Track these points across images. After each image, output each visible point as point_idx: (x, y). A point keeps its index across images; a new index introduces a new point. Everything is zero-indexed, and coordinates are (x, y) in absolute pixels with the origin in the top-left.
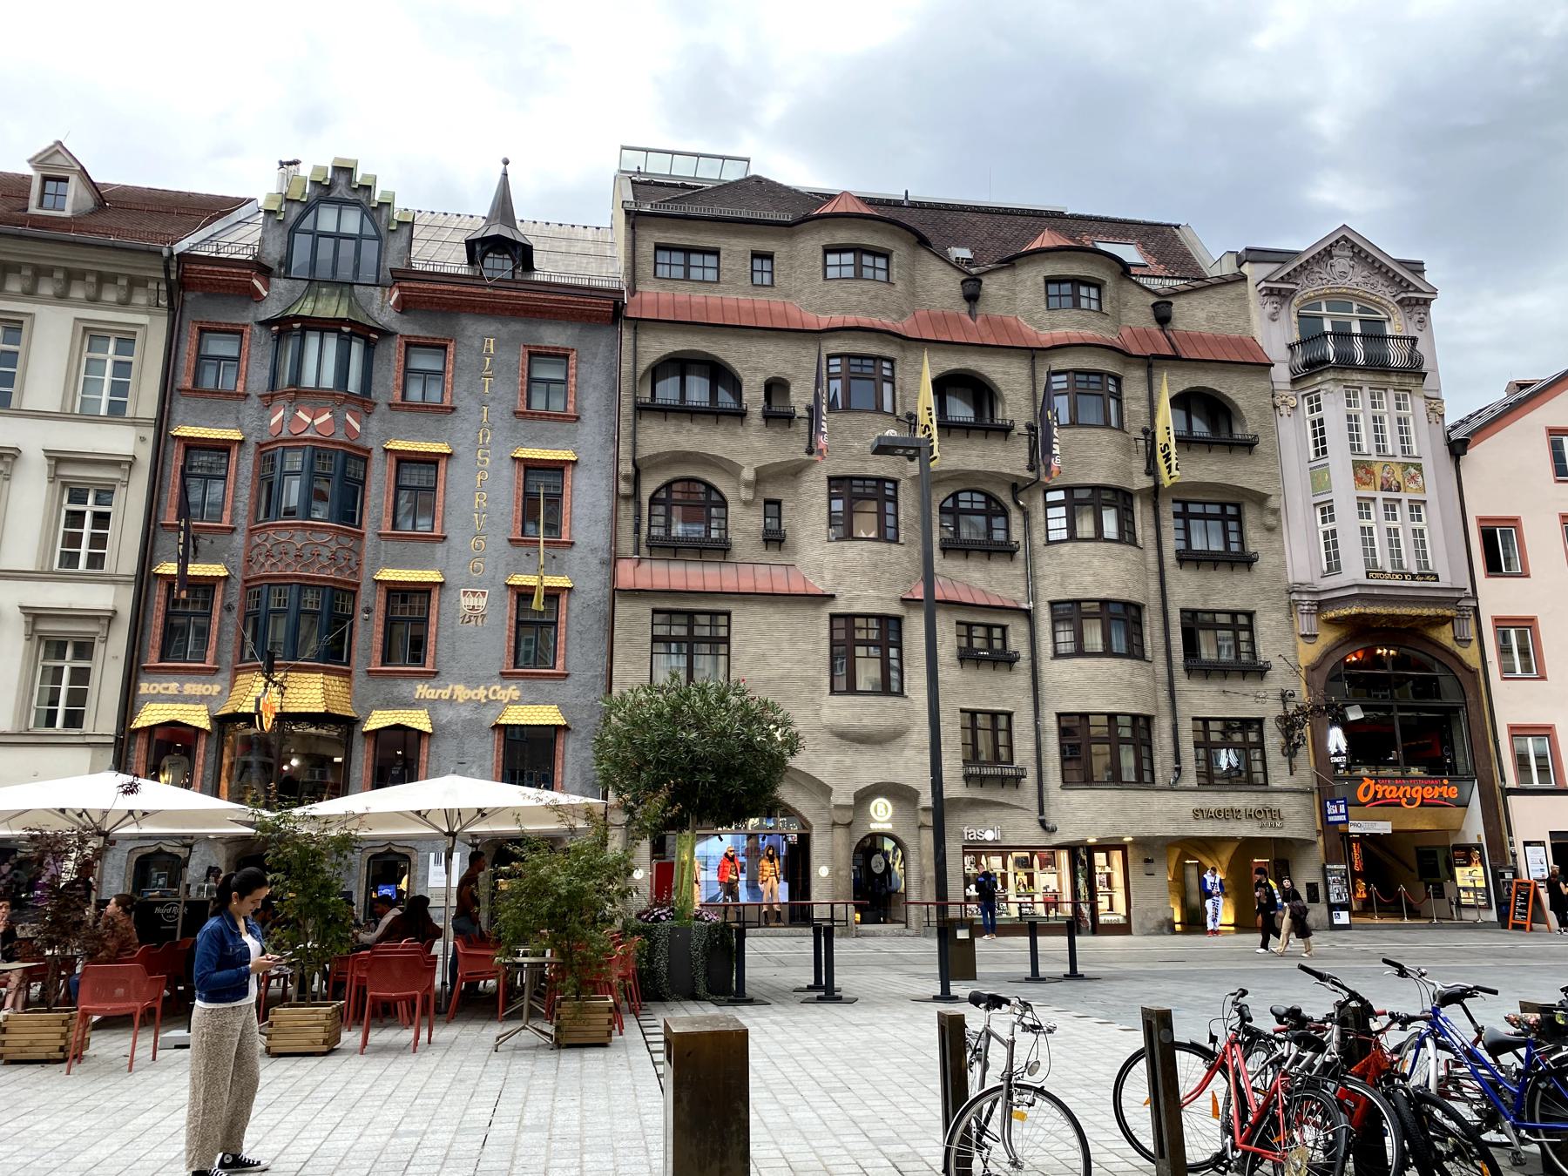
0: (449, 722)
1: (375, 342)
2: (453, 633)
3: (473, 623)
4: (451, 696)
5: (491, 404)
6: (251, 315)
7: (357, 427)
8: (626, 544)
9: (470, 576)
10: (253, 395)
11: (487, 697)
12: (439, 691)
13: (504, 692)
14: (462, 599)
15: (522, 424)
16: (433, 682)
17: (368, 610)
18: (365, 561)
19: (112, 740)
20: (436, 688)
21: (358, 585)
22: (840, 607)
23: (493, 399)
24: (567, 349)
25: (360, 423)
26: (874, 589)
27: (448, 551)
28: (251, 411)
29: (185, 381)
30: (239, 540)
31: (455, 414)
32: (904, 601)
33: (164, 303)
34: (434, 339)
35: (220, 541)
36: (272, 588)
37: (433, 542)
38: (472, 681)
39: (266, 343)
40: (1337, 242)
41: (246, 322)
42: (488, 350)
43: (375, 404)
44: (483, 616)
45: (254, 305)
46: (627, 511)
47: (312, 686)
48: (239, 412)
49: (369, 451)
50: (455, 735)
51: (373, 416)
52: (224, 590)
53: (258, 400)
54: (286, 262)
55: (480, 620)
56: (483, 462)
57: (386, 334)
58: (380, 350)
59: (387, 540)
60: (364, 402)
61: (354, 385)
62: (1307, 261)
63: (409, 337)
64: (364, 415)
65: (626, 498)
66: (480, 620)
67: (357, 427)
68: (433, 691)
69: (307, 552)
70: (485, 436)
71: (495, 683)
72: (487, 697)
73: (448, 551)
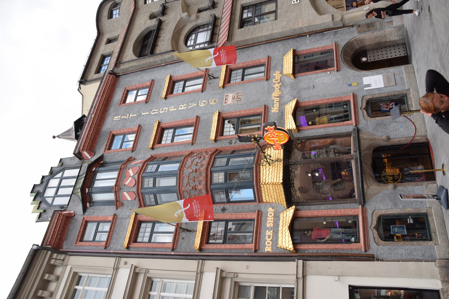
5: (141, 112)
19: (301, 262)
23: (139, 112)
24: (125, 90)
27: (204, 114)
31: (142, 125)
33: (62, 257)
42: (118, 118)
59: (196, 140)
70: (154, 112)
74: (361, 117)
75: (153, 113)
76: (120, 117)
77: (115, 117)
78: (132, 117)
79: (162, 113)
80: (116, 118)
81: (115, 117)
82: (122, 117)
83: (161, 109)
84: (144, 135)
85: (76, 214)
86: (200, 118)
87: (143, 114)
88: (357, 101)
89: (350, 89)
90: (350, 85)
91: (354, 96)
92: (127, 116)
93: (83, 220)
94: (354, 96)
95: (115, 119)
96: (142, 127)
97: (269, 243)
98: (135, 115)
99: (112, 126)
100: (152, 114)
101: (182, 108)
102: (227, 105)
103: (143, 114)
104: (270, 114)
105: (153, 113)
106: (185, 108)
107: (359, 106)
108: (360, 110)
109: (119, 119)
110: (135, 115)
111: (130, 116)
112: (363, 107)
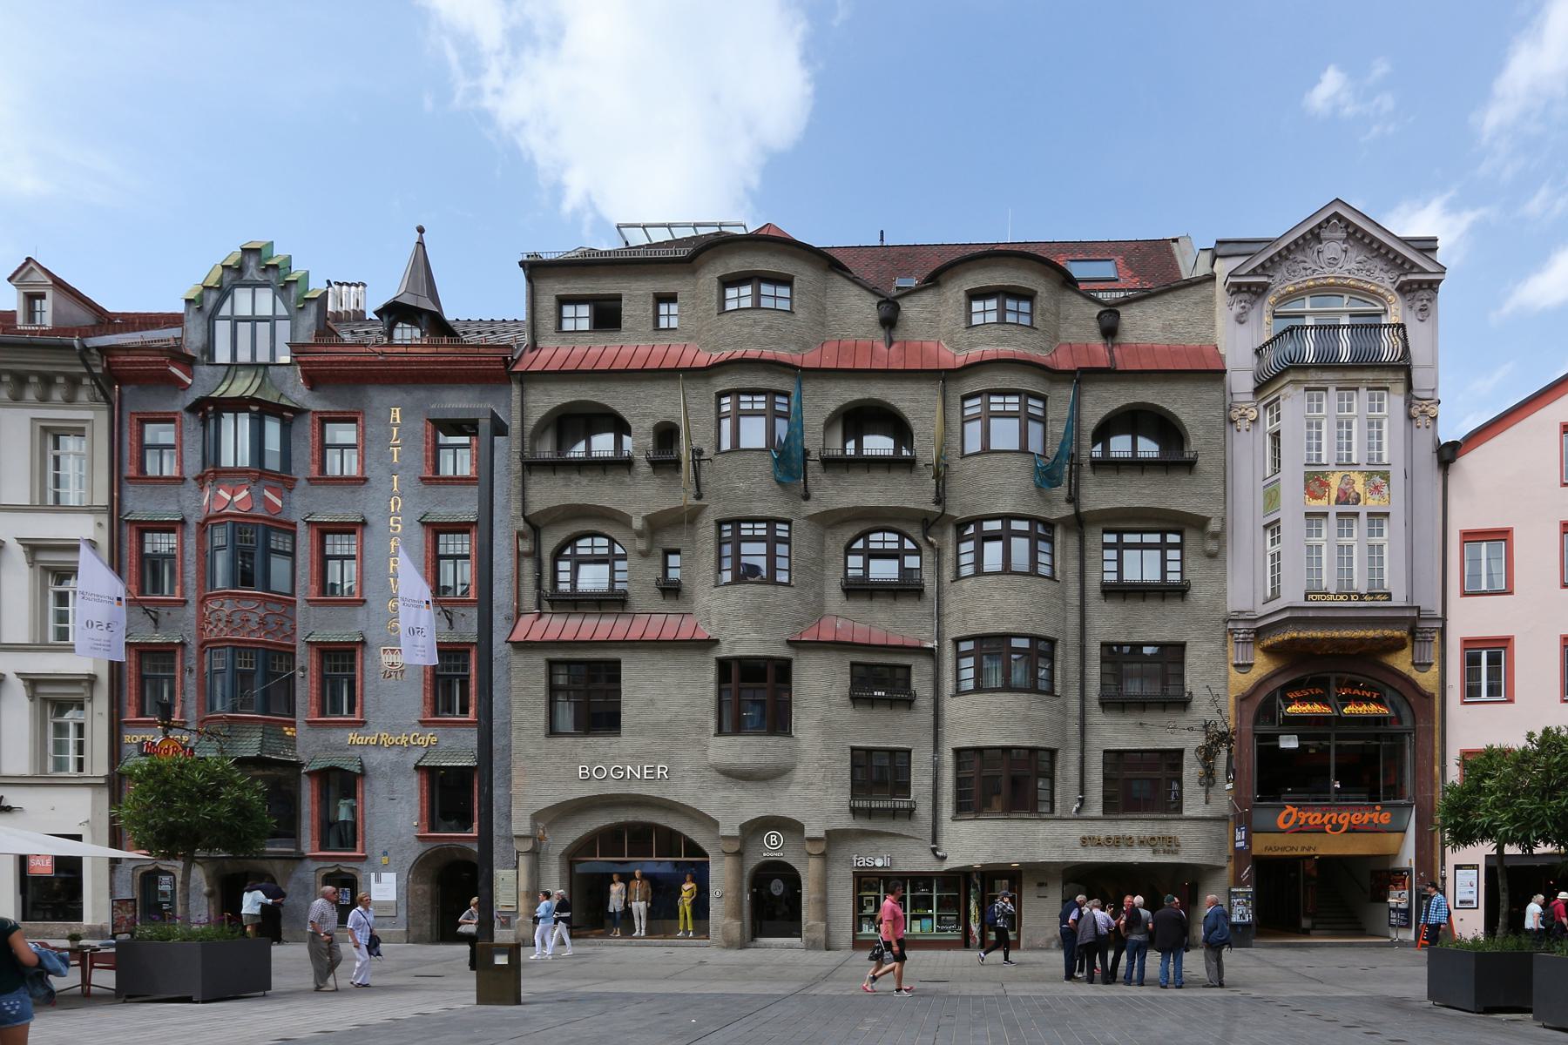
0: (379, 764)
1: (291, 421)
2: (378, 686)
3: (394, 677)
4: (378, 742)
5: (400, 472)
6: (180, 403)
7: (279, 503)
8: (529, 599)
9: (389, 636)
10: (190, 479)
11: (408, 742)
12: (367, 738)
13: (423, 739)
14: (383, 656)
15: (429, 490)
16: (362, 731)
17: (303, 669)
18: (297, 626)
20: (365, 735)
21: (294, 647)
22: (724, 651)
23: (401, 468)
25: (281, 498)
26: (756, 632)
27: (368, 613)
28: (190, 494)
29: (130, 470)
30: (191, 611)
31: (367, 485)
32: (789, 642)
34: (344, 413)
35: (176, 613)
36: (214, 651)
37: (354, 606)
38: (394, 729)
39: (195, 429)
40: (1328, 220)
41: (176, 410)
42: (395, 420)
43: (296, 480)
44: (403, 671)
45: (182, 393)
46: (528, 566)
47: (253, 734)
48: (179, 495)
49: (294, 525)
50: (384, 775)
51: (294, 491)
52: (182, 655)
53: (194, 483)
54: (209, 349)
55: (399, 674)
56: (396, 529)
57: (299, 412)
58: (297, 427)
59: (314, 605)
60: (283, 478)
61: (273, 463)
62: (1287, 248)
63: (321, 412)
64: (285, 492)
65: (527, 555)
66: (399, 674)
67: (279, 503)
68: (362, 738)
69: (237, 618)
70: (396, 504)
71: (416, 731)
72: (408, 742)
73: (368, 613)
74: (322, 864)
75: (392, 502)
76: (398, 421)
77: (398, 410)
78: (392, 453)
79: (389, 522)
80: (396, 414)
81: (398, 410)
82: (395, 429)
83: (400, 518)
84: (345, 494)
85: (187, 391)
86: (361, 605)
87: (395, 478)
88: (353, 861)
89: (378, 853)
90: (385, 853)
91: (364, 858)
92: (396, 440)
93: (176, 413)
94: (364, 858)
95: (395, 411)
96: (363, 484)
97: (135, 739)
98: (395, 460)
99: (377, 408)
100: (390, 500)
101: (392, 565)
102: (380, 653)
103: (395, 478)
104: (347, 730)
105: (392, 502)
106: (392, 572)
107: (343, 864)
108: (335, 863)
109: (391, 422)
110: (395, 460)
111: (395, 449)
112: (341, 869)
